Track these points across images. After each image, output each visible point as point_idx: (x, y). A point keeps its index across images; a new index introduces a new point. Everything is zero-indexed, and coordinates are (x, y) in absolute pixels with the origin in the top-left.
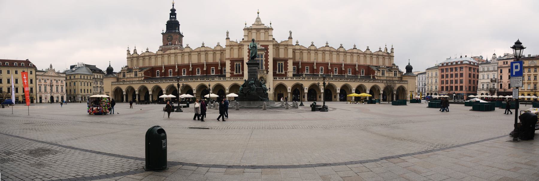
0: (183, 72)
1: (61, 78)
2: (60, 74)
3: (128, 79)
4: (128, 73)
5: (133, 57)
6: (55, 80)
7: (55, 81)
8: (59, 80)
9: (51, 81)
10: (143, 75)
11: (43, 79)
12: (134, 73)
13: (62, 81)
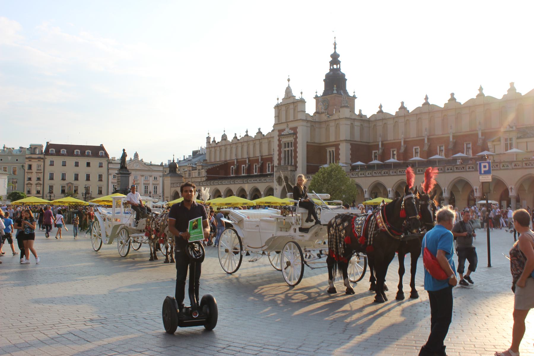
2: (151, 167)
3: (192, 179)
4: (193, 171)
8: (151, 176)
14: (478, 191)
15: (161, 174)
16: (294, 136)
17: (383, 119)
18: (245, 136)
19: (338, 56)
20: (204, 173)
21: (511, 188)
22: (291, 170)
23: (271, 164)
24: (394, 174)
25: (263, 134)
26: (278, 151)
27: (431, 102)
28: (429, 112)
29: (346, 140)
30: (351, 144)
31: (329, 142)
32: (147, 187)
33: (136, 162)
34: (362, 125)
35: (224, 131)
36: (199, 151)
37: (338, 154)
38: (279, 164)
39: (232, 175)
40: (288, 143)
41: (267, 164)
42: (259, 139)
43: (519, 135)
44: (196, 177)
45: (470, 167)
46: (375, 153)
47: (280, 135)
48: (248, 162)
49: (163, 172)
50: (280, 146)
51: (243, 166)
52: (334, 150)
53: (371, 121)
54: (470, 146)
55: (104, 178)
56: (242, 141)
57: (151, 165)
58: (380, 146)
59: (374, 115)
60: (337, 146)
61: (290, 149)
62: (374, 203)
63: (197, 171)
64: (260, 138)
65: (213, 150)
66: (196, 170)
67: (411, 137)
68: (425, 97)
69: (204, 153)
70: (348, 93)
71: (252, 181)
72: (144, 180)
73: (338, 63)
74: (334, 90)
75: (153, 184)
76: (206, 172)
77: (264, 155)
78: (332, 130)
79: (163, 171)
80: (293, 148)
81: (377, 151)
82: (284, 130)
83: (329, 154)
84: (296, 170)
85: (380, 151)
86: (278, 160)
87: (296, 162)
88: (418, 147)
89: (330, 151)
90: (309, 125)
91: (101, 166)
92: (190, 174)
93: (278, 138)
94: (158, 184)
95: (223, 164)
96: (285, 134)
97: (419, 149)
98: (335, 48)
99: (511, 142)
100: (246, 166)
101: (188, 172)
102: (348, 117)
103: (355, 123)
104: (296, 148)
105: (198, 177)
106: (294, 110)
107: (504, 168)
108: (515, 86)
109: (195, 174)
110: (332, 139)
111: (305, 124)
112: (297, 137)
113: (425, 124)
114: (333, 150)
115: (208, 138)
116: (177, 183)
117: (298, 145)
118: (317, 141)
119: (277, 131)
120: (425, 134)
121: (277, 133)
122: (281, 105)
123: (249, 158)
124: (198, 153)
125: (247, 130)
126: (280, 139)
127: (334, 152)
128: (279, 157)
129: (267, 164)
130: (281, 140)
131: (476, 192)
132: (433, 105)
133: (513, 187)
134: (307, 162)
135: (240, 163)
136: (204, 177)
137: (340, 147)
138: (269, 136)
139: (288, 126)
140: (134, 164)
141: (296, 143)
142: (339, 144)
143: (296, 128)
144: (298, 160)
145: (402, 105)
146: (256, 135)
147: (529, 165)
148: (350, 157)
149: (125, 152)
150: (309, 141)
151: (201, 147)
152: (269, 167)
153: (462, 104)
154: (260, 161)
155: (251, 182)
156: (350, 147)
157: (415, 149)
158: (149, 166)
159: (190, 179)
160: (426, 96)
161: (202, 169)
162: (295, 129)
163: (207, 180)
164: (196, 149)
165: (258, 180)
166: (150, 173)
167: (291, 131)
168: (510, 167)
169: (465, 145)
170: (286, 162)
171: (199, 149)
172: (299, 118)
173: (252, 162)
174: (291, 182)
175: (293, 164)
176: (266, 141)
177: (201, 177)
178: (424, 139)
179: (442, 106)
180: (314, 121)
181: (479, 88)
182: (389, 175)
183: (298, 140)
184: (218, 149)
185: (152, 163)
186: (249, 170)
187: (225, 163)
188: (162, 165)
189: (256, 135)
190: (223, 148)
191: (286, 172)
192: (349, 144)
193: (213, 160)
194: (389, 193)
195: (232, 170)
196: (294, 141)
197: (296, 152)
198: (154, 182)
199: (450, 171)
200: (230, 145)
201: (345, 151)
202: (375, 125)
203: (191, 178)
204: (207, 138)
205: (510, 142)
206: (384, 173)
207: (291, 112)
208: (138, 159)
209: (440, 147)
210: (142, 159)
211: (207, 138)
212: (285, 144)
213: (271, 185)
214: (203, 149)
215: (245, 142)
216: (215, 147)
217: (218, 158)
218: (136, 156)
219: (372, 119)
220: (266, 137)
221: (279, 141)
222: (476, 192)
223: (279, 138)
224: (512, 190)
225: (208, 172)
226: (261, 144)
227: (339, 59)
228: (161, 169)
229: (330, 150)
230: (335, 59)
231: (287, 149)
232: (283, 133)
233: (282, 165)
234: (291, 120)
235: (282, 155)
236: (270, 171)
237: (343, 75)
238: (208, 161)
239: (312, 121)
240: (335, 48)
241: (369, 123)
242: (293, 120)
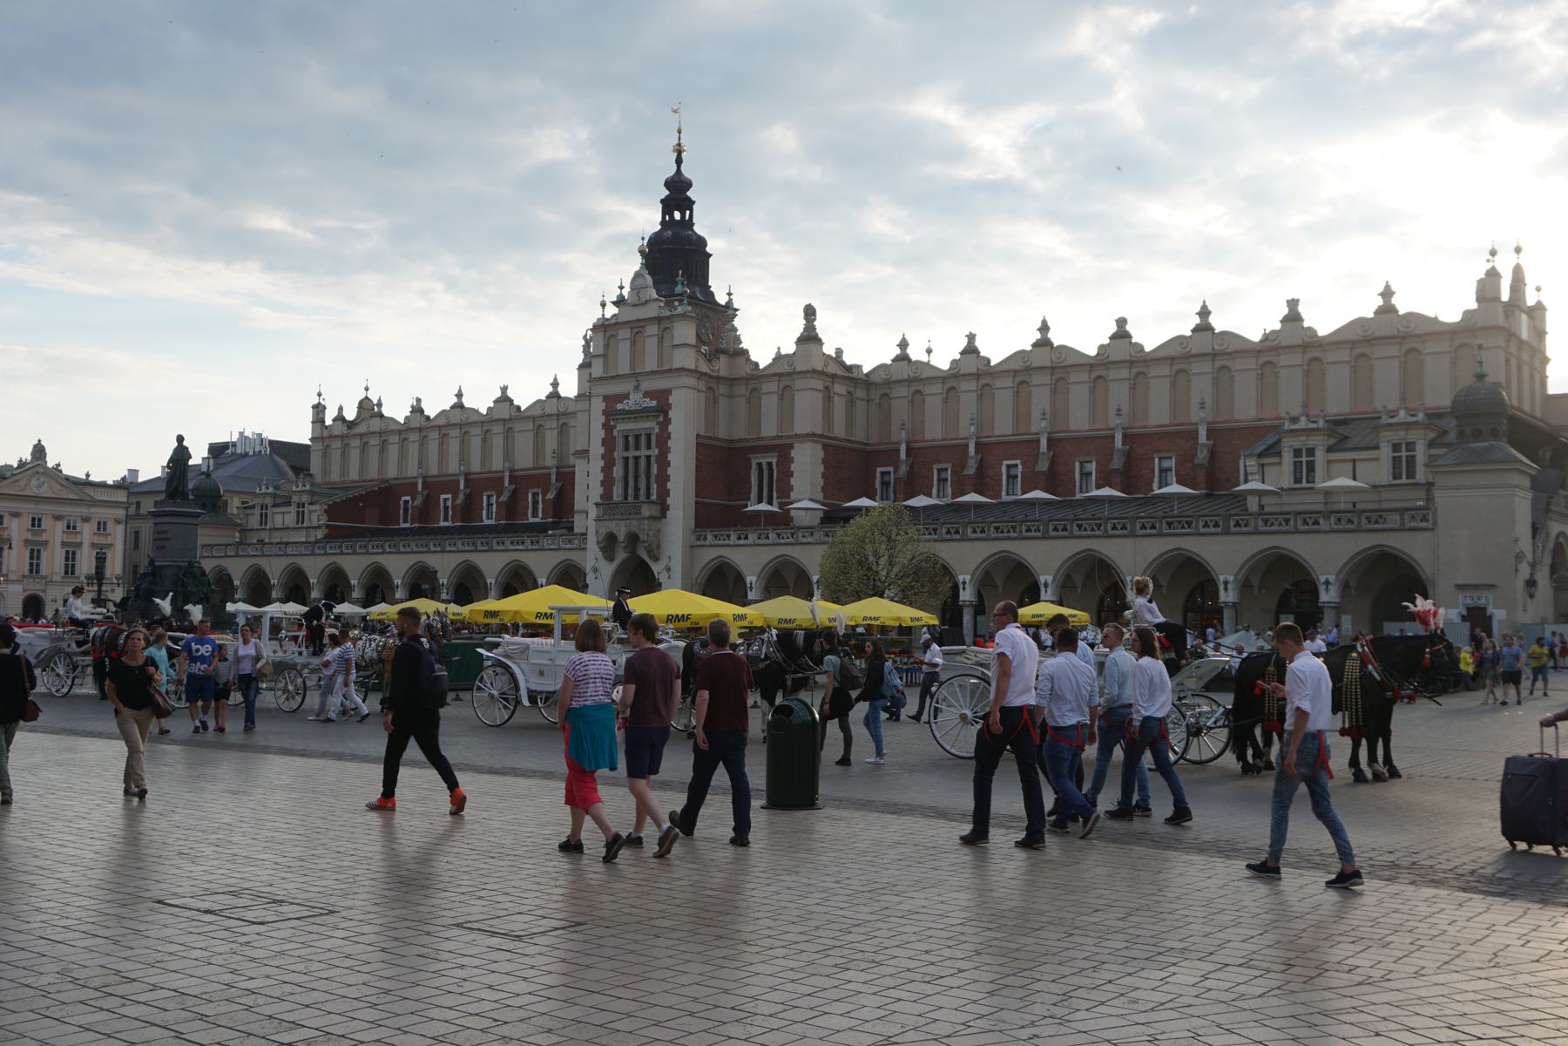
0: (485, 504)
1: (94, 510)
2: (89, 491)
3: (275, 534)
5: (332, 437)
6: (58, 518)
7: (60, 526)
8: (86, 520)
9: (36, 522)
10: (324, 520)
12: (293, 509)
13: (102, 526)
14: (1230, 586)
15: (121, 513)
16: (658, 416)
17: (910, 381)
18: (452, 407)
19: (689, 185)
20: (316, 515)
21: (1327, 582)
22: (651, 517)
23: (544, 496)
24: (979, 535)
25: (516, 403)
26: (603, 457)
27: (1057, 338)
28: (1053, 368)
29: (814, 435)
30: (825, 447)
31: (758, 439)
32: (74, 553)
33: (37, 472)
34: (849, 393)
35: (367, 389)
36: (234, 444)
37: (787, 474)
38: (607, 495)
39: (403, 525)
40: (637, 437)
41: (485, 497)
42: (504, 420)
43: (1332, 441)
44: (288, 528)
45: (1209, 523)
46: (883, 474)
47: (609, 413)
48: (465, 487)
49: (127, 509)
50: (608, 442)
51: (443, 496)
52: (774, 461)
53: (875, 384)
54: (1171, 463)
56: (443, 421)
57: (86, 483)
58: (903, 456)
59: (883, 366)
60: (783, 450)
61: (643, 452)
62: (1033, 616)
63: (293, 509)
64: (507, 416)
65: (336, 444)
66: (288, 504)
67: (998, 432)
68: (1039, 325)
69: (251, 453)
70: (712, 294)
71: (508, 542)
72: (63, 532)
73: (688, 204)
74: (676, 284)
75: (94, 545)
76: (325, 511)
77: (519, 465)
78: (770, 405)
79: (127, 503)
80: (655, 452)
81: (891, 469)
82: (627, 396)
83: (757, 473)
84: (664, 515)
85: (903, 469)
86: (602, 483)
87: (664, 493)
88: (1018, 462)
89: (760, 465)
90: (702, 386)
92: (264, 519)
93: (603, 419)
94: (110, 546)
95: (376, 488)
96: (627, 408)
97: (1020, 467)
98: (679, 161)
99: (1312, 459)
100: (454, 499)
101: (257, 511)
102: (820, 368)
103: (835, 385)
104: (664, 451)
105: (295, 528)
106: (661, 340)
107: (1238, 529)
108: (1302, 309)
109: (284, 518)
110: (769, 429)
111: (691, 381)
112: (668, 421)
113: (1041, 399)
114: (770, 460)
115: (319, 409)
116: (227, 545)
117: (670, 443)
118: (722, 433)
119: (601, 398)
120: (1039, 426)
121: (598, 406)
122: (617, 323)
123: (467, 475)
124: (229, 451)
125: (460, 390)
126: (612, 423)
127: (774, 467)
128: (604, 477)
129: (530, 496)
130: (615, 427)
131: (1226, 589)
132: (1062, 347)
133: (1332, 578)
134: (697, 496)
135: (435, 487)
136: (319, 527)
137: (793, 453)
138: (538, 412)
139: (637, 388)
140: (30, 480)
141: (664, 437)
142: (791, 446)
143: (668, 392)
144: (670, 485)
145: (969, 342)
146: (492, 405)
147: (1377, 522)
148: (821, 482)
149: (185, 443)
150: (702, 433)
151: (241, 434)
152: (535, 503)
153: (1148, 349)
154: (506, 484)
155: (502, 548)
156: (822, 454)
157: (1009, 467)
158: (81, 487)
159: (267, 534)
160: (1044, 323)
161: (311, 504)
162: (662, 396)
163: (326, 537)
164: (223, 438)
165: (508, 542)
166: (84, 511)
167: (648, 400)
168: (1323, 524)
169: (1157, 460)
170: (631, 491)
171: (235, 439)
172: (676, 365)
173: (477, 485)
174: (649, 551)
175: (654, 497)
176: (530, 426)
177: (307, 528)
178: (1038, 441)
179: (1093, 352)
180: (715, 374)
181: (1198, 310)
182: (965, 539)
183: (670, 428)
184: (356, 443)
185: (90, 479)
186: (468, 509)
187: (383, 486)
188: (127, 485)
189: (492, 405)
190: (374, 441)
191: (635, 522)
192: (819, 447)
193: (335, 476)
194: (964, 589)
195: (406, 510)
196: (657, 430)
197: (664, 463)
198: (96, 540)
199: (1149, 531)
200: (400, 432)
201: (807, 466)
202: (885, 395)
203: (270, 530)
204: (314, 407)
205: (1304, 455)
206: (948, 532)
207: (651, 345)
208: (46, 462)
209: (1082, 463)
210: (59, 465)
211: (314, 407)
212: (626, 437)
213: (575, 556)
214: (246, 438)
215: (454, 425)
216: (342, 437)
217: (358, 470)
218: (38, 455)
219: (876, 379)
220: (526, 414)
221: (607, 427)
222: (1226, 589)
223: (607, 420)
224: (1330, 587)
225: (333, 511)
226: (508, 433)
227: (689, 193)
228: (122, 497)
229: (764, 461)
230: (677, 195)
231: (632, 453)
232: (619, 406)
233: (615, 498)
234: (648, 369)
235: (618, 471)
236: (540, 515)
237: (702, 242)
238: (318, 478)
239: (711, 377)
240: (679, 161)
241: (868, 390)
242: (655, 369)
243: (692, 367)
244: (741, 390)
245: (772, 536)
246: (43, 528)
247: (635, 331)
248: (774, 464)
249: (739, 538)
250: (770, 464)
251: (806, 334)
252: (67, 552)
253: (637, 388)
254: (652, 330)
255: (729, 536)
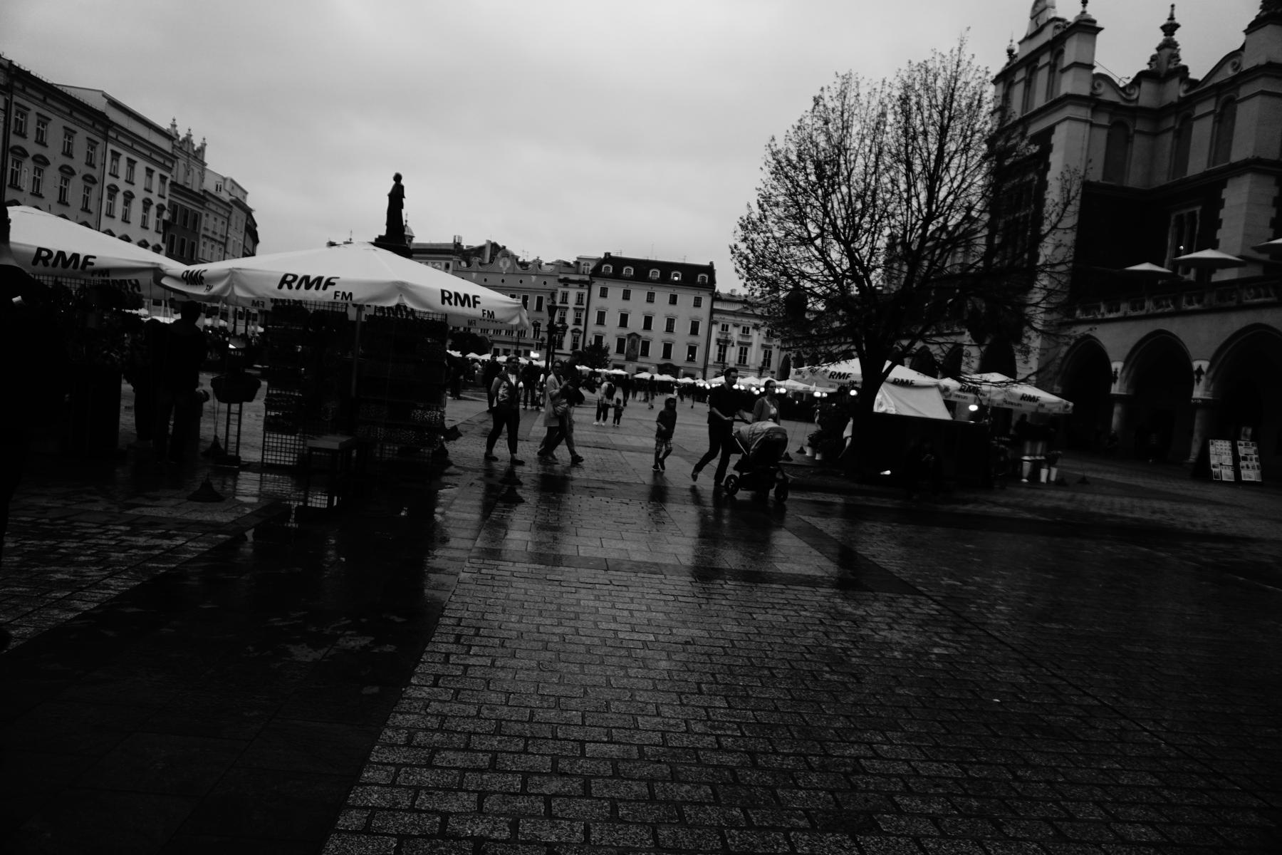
11: (736, 326)
52: (1198, 209)
55: (702, 329)
91: (697, 303)
106: (1053, 67)
110: (1197, 164)
111: (1084, 113)
114: (1191, 210)
137: (1226, 194)
143: (1050, 130)
150: (1096, 176)
192: (1272, 181)
243: (1085, 90)
244: (1171, 122)
245: (1149, 305)
246: (729, 331)
247: (1030, 69)
248: (1198, 213)
249: (1110, 311)
250: (1194, 214)
251: (1265, 13)
252: (741, 349)
253: (1023, 135)
254: (1045, 59)
255: (1099, 309)
